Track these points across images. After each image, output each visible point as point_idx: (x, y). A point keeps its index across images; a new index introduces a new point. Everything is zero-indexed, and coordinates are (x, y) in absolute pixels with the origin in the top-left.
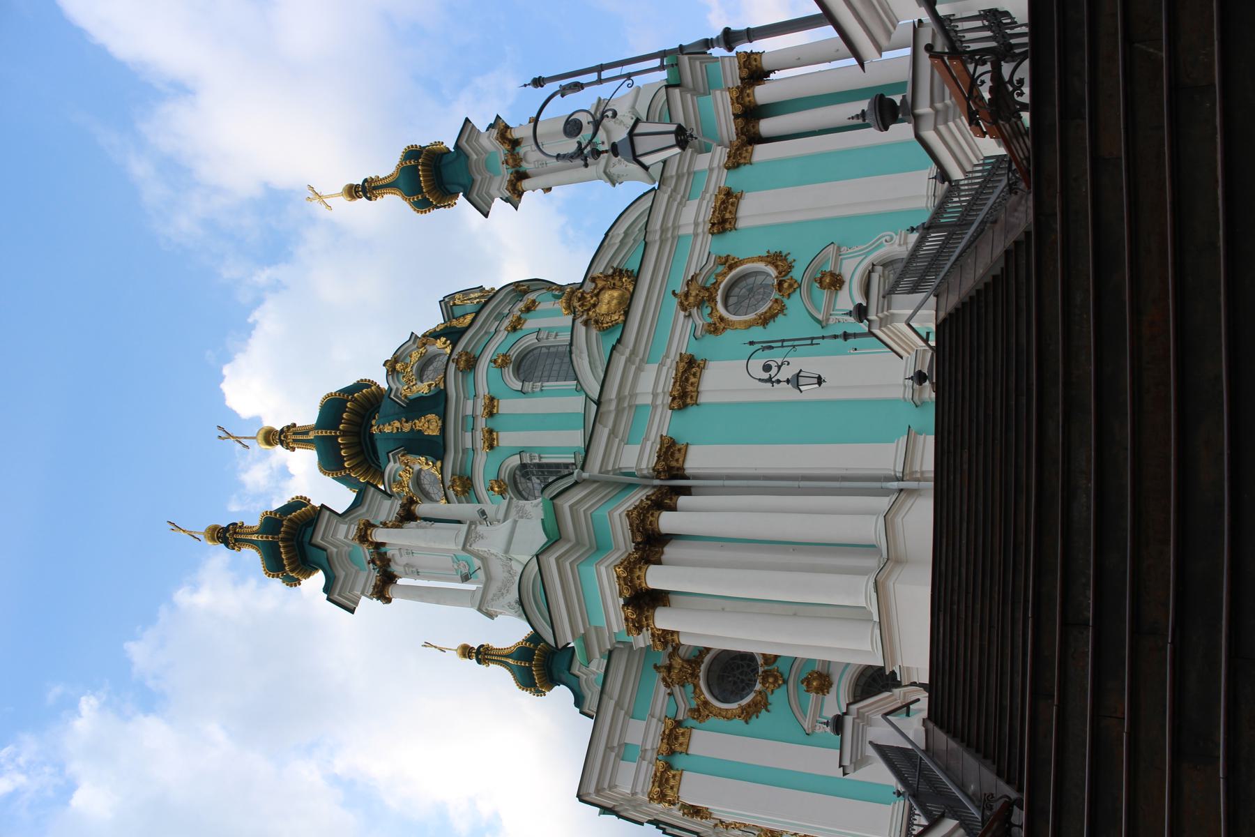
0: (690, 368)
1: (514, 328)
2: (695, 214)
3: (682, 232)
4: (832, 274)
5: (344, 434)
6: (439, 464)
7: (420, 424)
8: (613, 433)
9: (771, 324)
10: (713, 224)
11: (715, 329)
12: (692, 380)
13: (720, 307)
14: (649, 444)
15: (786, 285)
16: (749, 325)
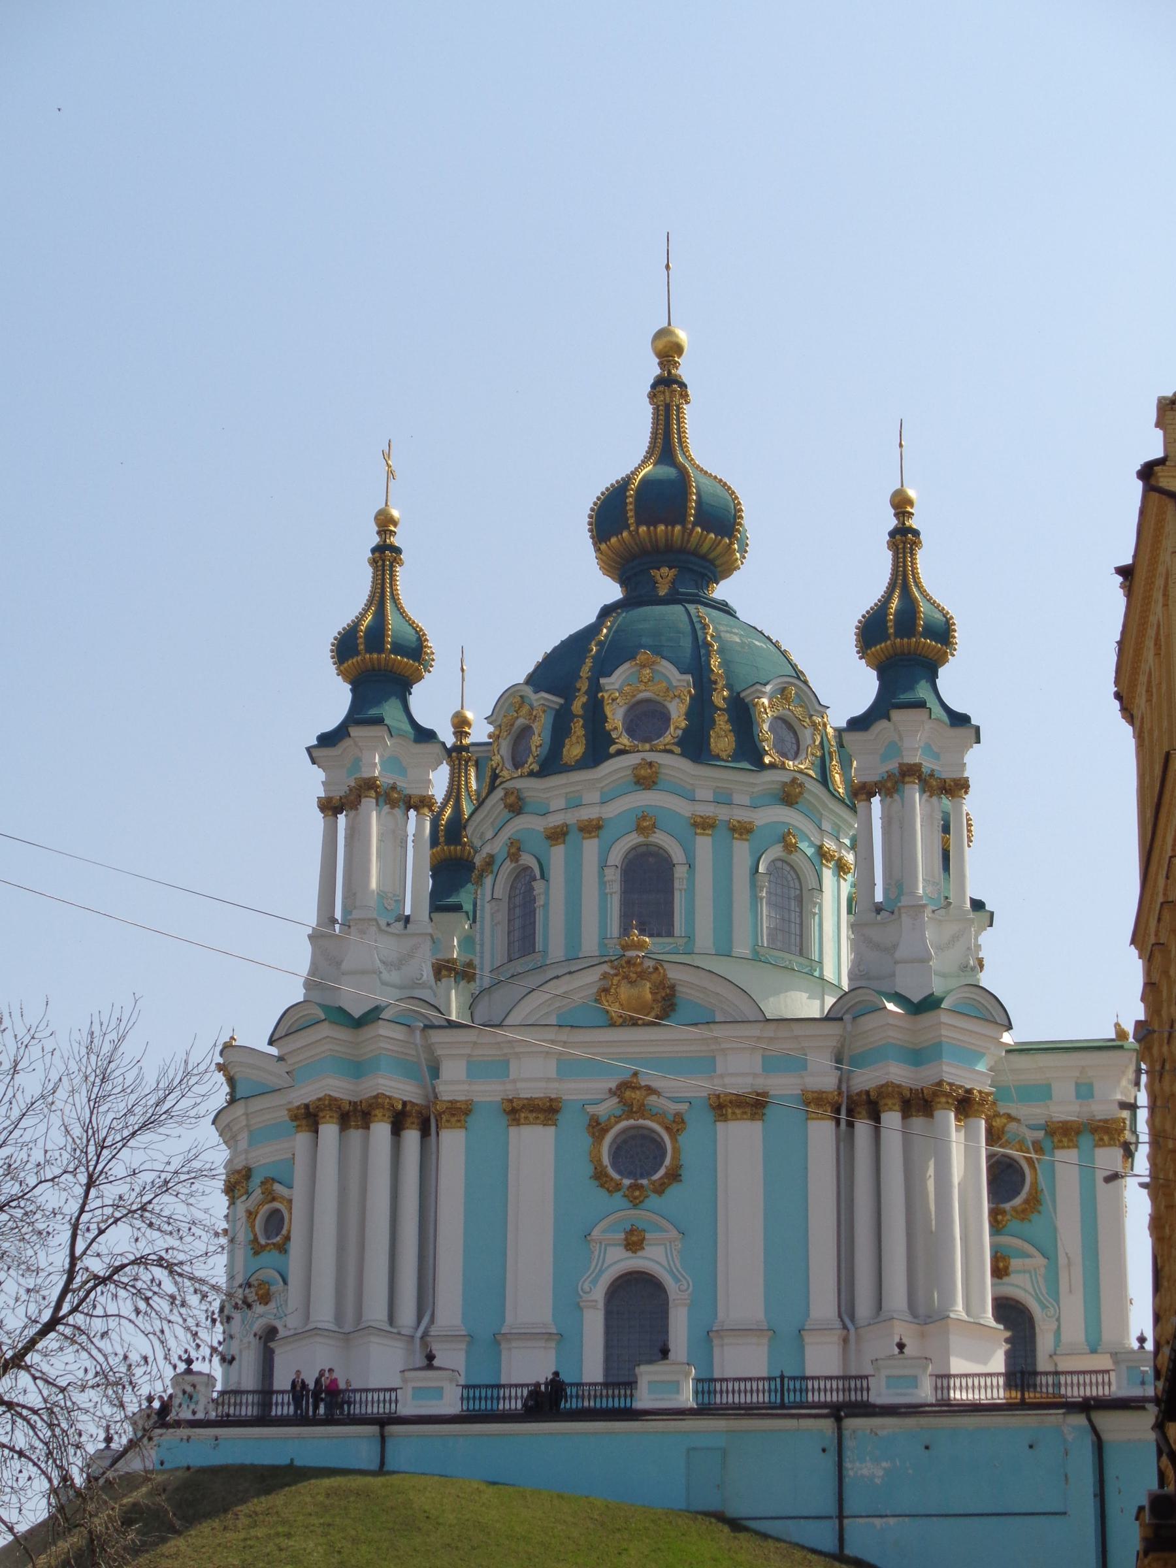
0: (547, 1111)
1: (704, 825)
2: (739, 1072)
3: (719, 1059)
4: (644, 1238)
5: (634, 535)
6: (536, 767)
7: (578, 728)
8: (475, 1043)
9: (596, 1183)
10: (718, 1096)
11: (597, 1128)
12: (532, 1116)
13: (624, 1124)
14: (466, 1087)
15: (637, 1193)
16: (596, 1161)
